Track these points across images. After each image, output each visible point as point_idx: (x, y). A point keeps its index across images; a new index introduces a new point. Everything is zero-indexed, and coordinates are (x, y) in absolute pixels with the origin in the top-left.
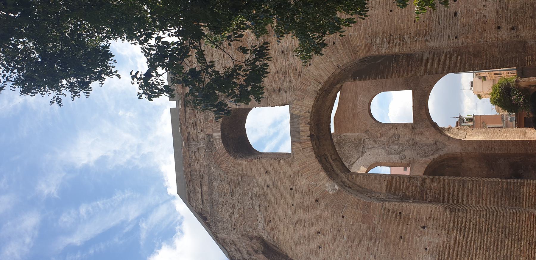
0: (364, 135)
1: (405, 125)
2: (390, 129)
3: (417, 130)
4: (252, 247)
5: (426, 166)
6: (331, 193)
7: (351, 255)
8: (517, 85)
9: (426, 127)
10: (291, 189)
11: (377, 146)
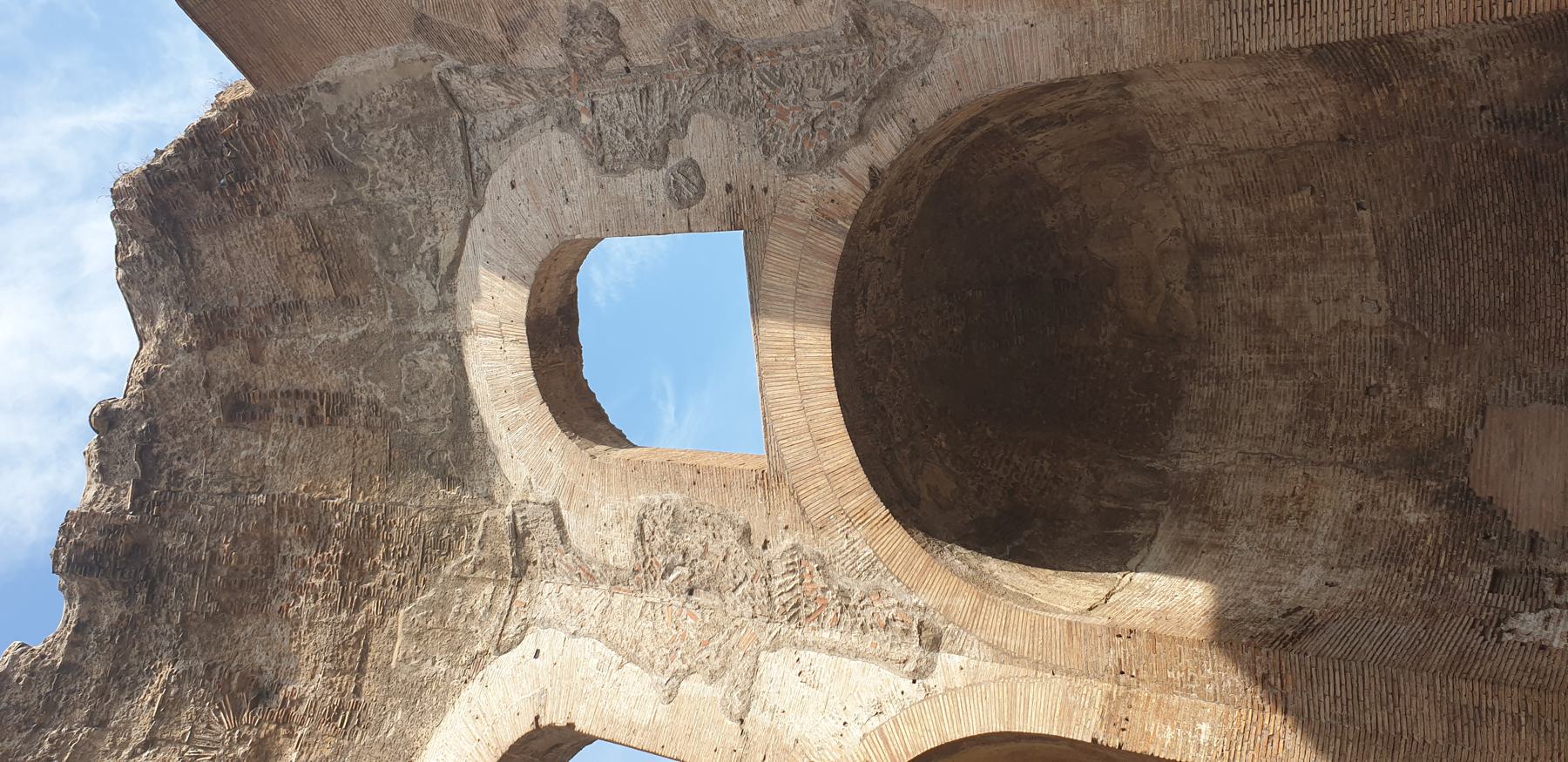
5: (834, 245)
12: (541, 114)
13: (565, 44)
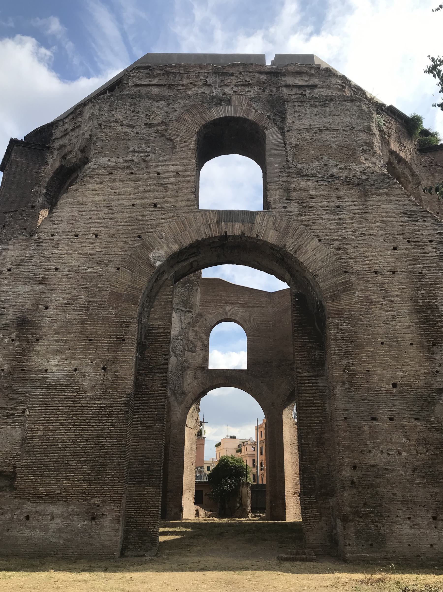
0: (197, 312)
1: (206, 360)
2: (202, 341)
3: (199, 373)
4: (71, 152)
6: (151, 256)
7: (67, 276)
8: (243, 484)
9: (203, 383)
10: (155, 205)
11: (183, 325)
12: (182, 328)
13: (192, 341)
